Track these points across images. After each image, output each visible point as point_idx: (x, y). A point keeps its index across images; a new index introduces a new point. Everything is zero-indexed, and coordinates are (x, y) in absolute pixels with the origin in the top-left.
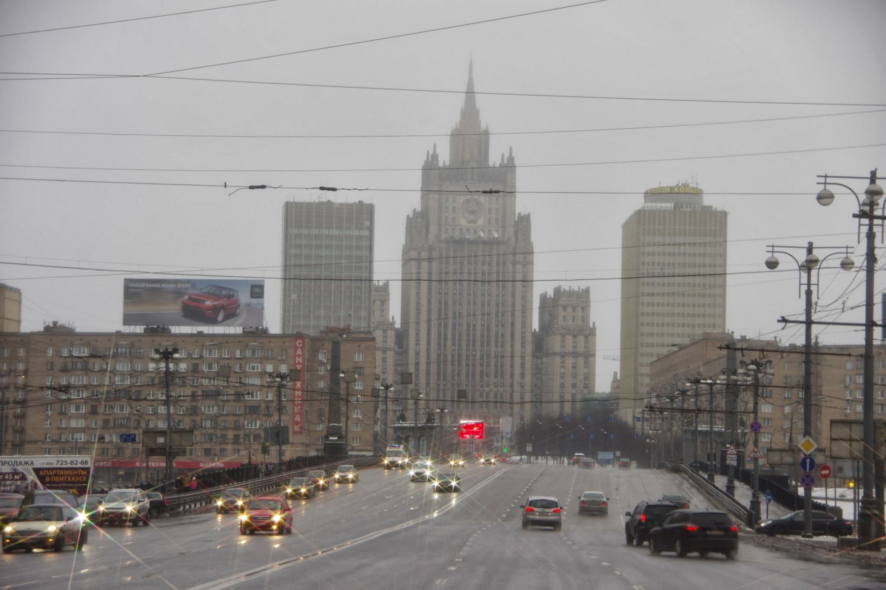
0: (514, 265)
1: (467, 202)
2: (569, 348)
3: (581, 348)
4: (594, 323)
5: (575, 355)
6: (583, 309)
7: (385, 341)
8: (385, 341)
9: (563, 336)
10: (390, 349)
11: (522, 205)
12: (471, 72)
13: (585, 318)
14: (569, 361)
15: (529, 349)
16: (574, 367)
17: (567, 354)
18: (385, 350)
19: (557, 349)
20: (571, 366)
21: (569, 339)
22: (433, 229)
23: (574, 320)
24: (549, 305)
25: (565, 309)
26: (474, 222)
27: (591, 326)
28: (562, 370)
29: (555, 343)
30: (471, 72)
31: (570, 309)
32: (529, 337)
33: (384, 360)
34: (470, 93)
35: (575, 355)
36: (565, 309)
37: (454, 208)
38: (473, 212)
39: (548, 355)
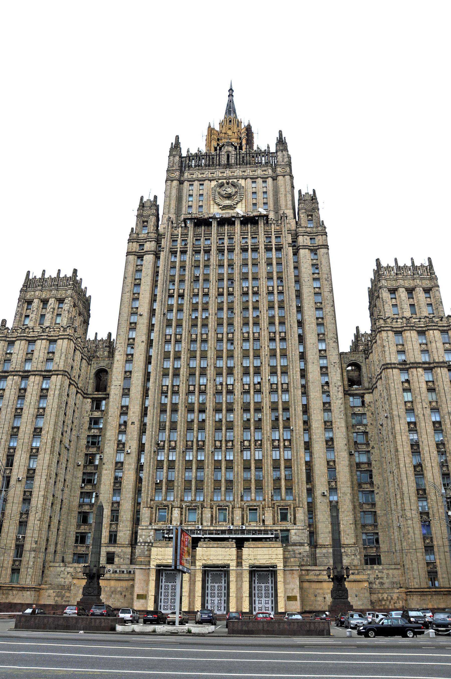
1: (222, 185)
2: (415, 354)
6: (427, 291)
10: (56, 373)
11: (303, 183)
12: (231, 95)
14: (420, 378)
15: (335, 377)
16: (431, 390)
18: (46, 375)
20: (424, 386)
21: (411, 337)
25: (393, 291)
26: (231, 207)
28: (408, 397)
29: (388, 349)
30: (231, 95)
31: (402, 294)
32: (334, 358)
33: (43, 394)
35: (429, 367)
36: (393, 291)
38: (229, 197)
39: (372, 389)
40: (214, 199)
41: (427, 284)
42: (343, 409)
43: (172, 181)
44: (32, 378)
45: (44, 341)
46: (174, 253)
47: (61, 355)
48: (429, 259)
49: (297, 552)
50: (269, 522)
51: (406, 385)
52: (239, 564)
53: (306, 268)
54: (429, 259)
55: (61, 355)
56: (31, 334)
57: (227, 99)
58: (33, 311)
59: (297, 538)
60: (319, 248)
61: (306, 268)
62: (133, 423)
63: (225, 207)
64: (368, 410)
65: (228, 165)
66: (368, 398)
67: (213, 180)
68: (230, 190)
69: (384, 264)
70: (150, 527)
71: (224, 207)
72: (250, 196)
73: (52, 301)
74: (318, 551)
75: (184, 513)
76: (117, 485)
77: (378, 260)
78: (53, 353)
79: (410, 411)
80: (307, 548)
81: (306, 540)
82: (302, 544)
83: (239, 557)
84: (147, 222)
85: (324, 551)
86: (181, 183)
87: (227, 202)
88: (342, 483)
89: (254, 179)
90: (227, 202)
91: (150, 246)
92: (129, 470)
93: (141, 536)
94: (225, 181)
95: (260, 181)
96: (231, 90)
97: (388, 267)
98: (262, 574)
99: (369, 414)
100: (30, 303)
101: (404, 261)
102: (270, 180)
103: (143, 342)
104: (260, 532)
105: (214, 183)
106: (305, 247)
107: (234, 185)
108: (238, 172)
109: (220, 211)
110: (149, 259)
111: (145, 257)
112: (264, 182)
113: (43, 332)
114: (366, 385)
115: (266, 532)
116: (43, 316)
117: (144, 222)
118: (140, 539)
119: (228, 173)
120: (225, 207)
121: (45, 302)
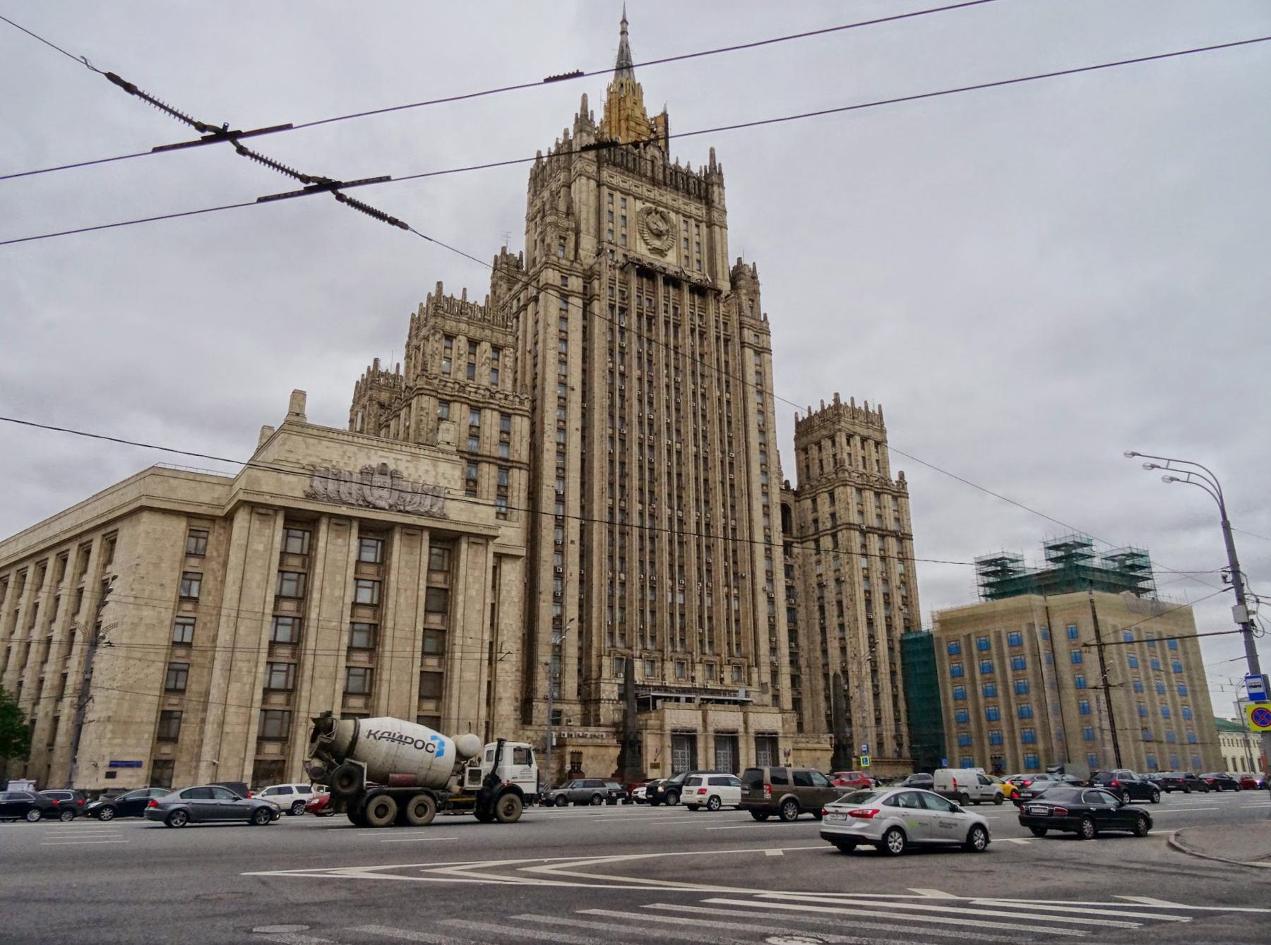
0: (742, 347)
3: (892, 525)
4: (902, 475)
5: (883, 534)
6: (877, 444)
7: (505, 443)
8: (505, 443)
9: (859, 491)
12: (624, 32)
13: (882, 464)
14: (874, 543)
17: (871, 530)
19: (855, 518)
21: (869, 495)
22: (588, 243)
23: (865, 467)
24: (810, 431)
25: (849, 437)
26: (661, 252)
27: (894, 477)
32: (776, 498)
34: (624, 65)
36: (849, 437)
37: (624, 217)
38: (659, 235)
40: (641, 233)
41: (878, 436)
43: (589, 178)
44: (485, 468)
45: (495, 413)
46: (612, 307)
48: (880, 407)
50: (727, 681)
52: (746, 728)
54: (880, 407)
56: (472, 396)
57: (618, 38)
58: (461, 355)
60: (762, 351)
62: (572, 542)
63: (655, 250)
65: (654, 182)
66: (796, 549)
67: (640, 199)
68: (663, 227)
69: (842, 402)
71: (655, 249)
72: (683, 244)
73: (485, 346)
77: (837, 394)
78: (508, 433)
79: (867, 578)
83: (745, 722)
84: (565, 239)
86: (599, 185)
87: (657, 243)
89: (687, 216)
90: (657, 243)
91: (575, 283)
94: (653, 206)
95: (692, 222)
96: (624, 21)
97: (846, 406)
98: (767, 741)
99: (796, 566)
100: (449, 337)
101: (859, 404)
102: (703, 226)
104: (718, 692)
105: (639, 205)
106: (750, 346)
107: (664, 218)
108: (668, 197)
109: (648, 253)
110: (577, 301)
111: (571, 300)
112: (697, 226)
113: (491, 397)
114: (795, 532)
115: (725, 692)
116: (471, 366)
117: (561, 237)
119: (655, 193)
120: (655, 250)
121: (473, 343)
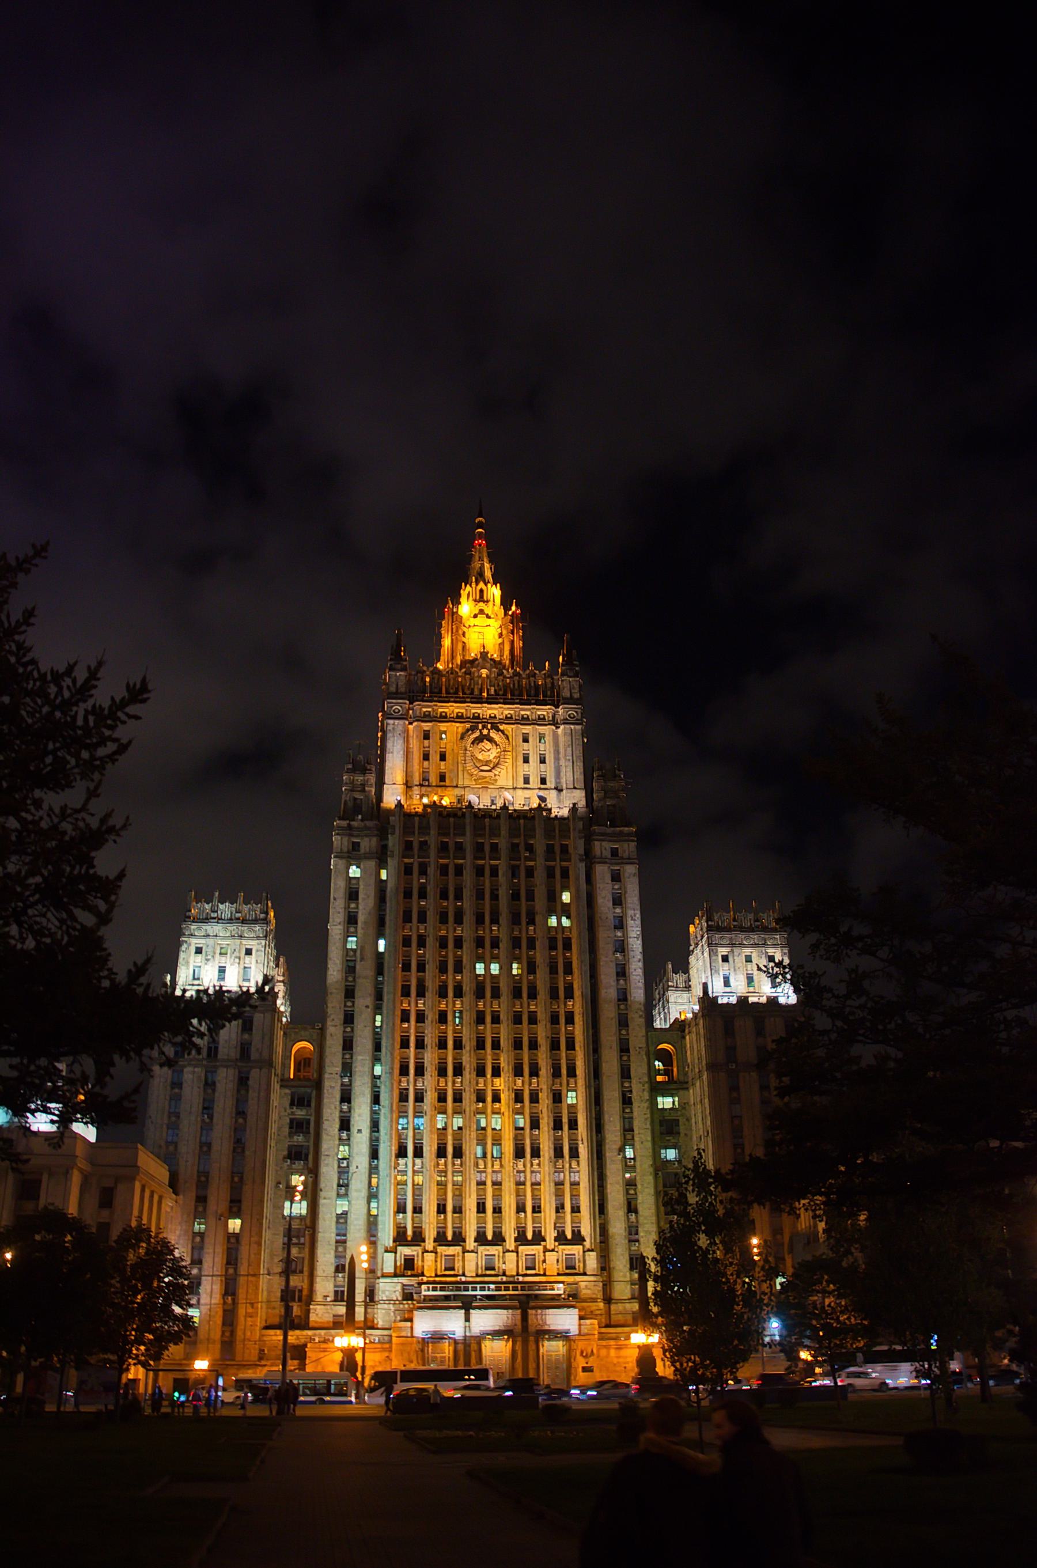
42: (649, 1115)
47: (263, 1038)
49: (588, 1310)
51: (735, 1095)
53: (604, 898)
55: (263, 1038)
59: (589, 1292)
61: (604, 898)
62: (359, 1131)
64: (682, 1115)
70: (395, 1280)
74: (613, 1307)
75: (439, 1260)
76: (342, 1221)
80: (601, 1305)
81: (600, 1295)
82: (594, 1300)
85: (620, 1307)
88: (645, 1218)
92: (357, 1199)
93: (384, 1292)
103: (367, 1007)
118: (380, 1296)
